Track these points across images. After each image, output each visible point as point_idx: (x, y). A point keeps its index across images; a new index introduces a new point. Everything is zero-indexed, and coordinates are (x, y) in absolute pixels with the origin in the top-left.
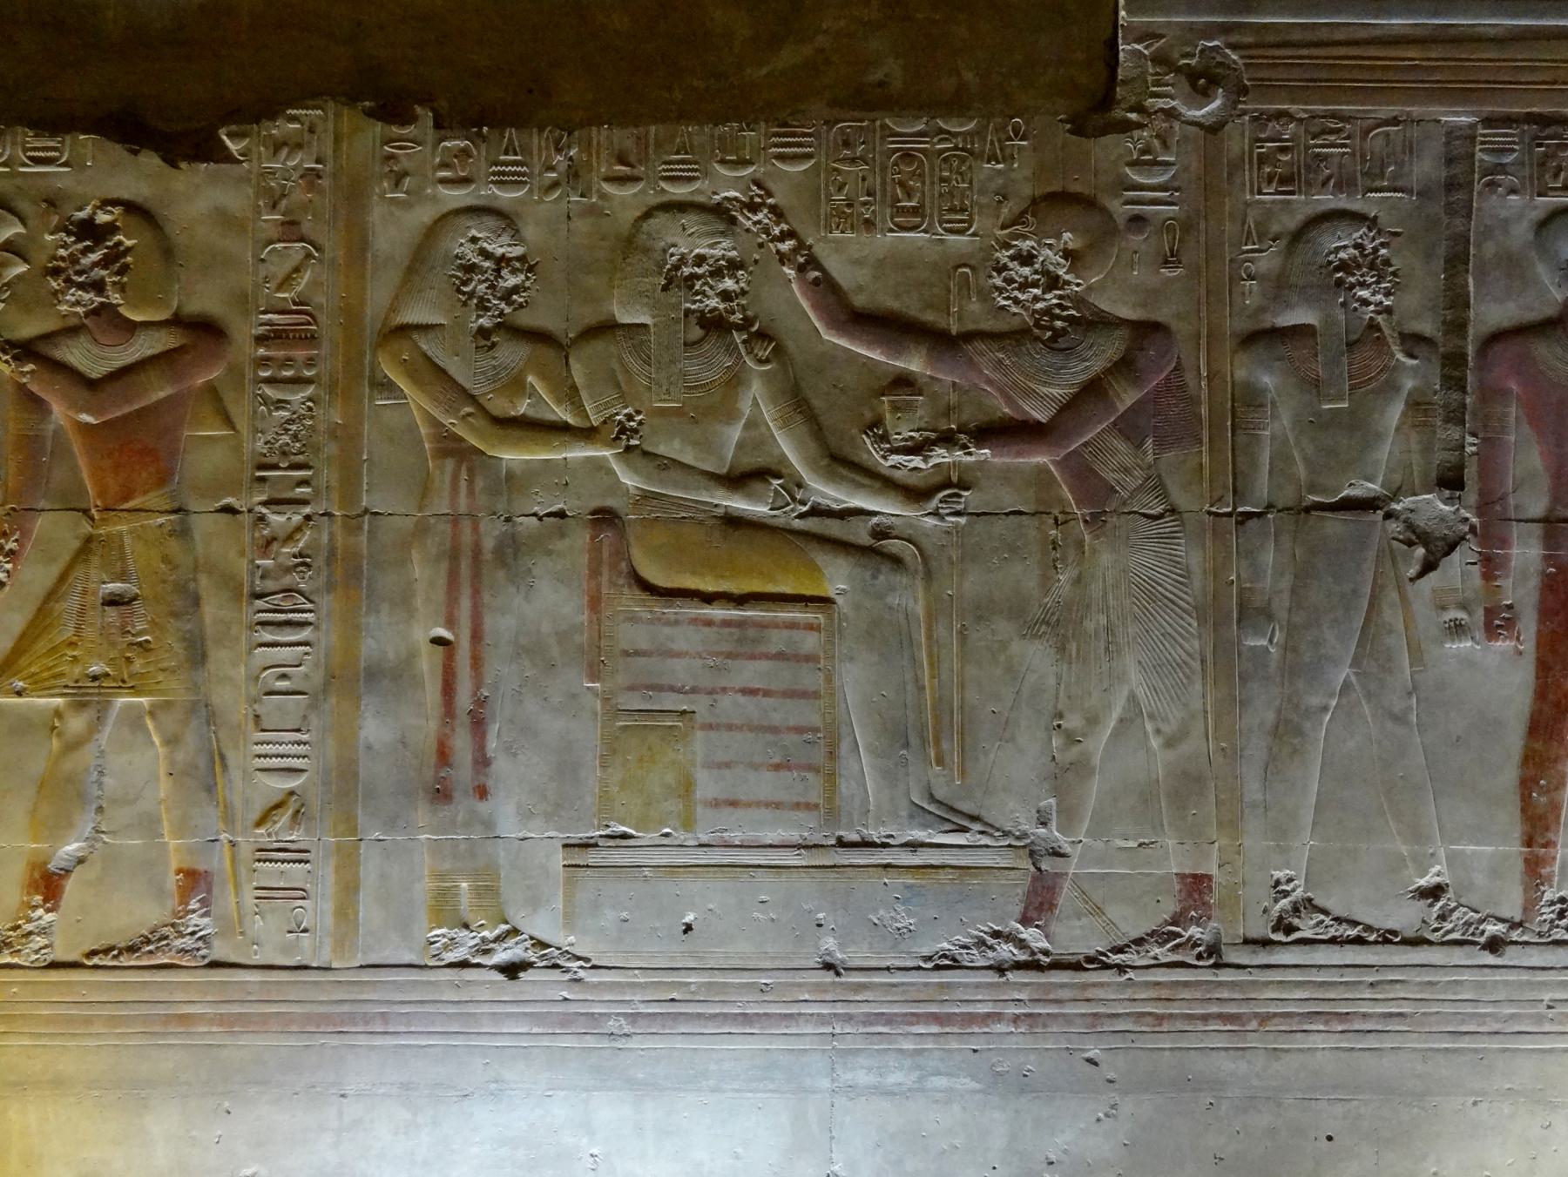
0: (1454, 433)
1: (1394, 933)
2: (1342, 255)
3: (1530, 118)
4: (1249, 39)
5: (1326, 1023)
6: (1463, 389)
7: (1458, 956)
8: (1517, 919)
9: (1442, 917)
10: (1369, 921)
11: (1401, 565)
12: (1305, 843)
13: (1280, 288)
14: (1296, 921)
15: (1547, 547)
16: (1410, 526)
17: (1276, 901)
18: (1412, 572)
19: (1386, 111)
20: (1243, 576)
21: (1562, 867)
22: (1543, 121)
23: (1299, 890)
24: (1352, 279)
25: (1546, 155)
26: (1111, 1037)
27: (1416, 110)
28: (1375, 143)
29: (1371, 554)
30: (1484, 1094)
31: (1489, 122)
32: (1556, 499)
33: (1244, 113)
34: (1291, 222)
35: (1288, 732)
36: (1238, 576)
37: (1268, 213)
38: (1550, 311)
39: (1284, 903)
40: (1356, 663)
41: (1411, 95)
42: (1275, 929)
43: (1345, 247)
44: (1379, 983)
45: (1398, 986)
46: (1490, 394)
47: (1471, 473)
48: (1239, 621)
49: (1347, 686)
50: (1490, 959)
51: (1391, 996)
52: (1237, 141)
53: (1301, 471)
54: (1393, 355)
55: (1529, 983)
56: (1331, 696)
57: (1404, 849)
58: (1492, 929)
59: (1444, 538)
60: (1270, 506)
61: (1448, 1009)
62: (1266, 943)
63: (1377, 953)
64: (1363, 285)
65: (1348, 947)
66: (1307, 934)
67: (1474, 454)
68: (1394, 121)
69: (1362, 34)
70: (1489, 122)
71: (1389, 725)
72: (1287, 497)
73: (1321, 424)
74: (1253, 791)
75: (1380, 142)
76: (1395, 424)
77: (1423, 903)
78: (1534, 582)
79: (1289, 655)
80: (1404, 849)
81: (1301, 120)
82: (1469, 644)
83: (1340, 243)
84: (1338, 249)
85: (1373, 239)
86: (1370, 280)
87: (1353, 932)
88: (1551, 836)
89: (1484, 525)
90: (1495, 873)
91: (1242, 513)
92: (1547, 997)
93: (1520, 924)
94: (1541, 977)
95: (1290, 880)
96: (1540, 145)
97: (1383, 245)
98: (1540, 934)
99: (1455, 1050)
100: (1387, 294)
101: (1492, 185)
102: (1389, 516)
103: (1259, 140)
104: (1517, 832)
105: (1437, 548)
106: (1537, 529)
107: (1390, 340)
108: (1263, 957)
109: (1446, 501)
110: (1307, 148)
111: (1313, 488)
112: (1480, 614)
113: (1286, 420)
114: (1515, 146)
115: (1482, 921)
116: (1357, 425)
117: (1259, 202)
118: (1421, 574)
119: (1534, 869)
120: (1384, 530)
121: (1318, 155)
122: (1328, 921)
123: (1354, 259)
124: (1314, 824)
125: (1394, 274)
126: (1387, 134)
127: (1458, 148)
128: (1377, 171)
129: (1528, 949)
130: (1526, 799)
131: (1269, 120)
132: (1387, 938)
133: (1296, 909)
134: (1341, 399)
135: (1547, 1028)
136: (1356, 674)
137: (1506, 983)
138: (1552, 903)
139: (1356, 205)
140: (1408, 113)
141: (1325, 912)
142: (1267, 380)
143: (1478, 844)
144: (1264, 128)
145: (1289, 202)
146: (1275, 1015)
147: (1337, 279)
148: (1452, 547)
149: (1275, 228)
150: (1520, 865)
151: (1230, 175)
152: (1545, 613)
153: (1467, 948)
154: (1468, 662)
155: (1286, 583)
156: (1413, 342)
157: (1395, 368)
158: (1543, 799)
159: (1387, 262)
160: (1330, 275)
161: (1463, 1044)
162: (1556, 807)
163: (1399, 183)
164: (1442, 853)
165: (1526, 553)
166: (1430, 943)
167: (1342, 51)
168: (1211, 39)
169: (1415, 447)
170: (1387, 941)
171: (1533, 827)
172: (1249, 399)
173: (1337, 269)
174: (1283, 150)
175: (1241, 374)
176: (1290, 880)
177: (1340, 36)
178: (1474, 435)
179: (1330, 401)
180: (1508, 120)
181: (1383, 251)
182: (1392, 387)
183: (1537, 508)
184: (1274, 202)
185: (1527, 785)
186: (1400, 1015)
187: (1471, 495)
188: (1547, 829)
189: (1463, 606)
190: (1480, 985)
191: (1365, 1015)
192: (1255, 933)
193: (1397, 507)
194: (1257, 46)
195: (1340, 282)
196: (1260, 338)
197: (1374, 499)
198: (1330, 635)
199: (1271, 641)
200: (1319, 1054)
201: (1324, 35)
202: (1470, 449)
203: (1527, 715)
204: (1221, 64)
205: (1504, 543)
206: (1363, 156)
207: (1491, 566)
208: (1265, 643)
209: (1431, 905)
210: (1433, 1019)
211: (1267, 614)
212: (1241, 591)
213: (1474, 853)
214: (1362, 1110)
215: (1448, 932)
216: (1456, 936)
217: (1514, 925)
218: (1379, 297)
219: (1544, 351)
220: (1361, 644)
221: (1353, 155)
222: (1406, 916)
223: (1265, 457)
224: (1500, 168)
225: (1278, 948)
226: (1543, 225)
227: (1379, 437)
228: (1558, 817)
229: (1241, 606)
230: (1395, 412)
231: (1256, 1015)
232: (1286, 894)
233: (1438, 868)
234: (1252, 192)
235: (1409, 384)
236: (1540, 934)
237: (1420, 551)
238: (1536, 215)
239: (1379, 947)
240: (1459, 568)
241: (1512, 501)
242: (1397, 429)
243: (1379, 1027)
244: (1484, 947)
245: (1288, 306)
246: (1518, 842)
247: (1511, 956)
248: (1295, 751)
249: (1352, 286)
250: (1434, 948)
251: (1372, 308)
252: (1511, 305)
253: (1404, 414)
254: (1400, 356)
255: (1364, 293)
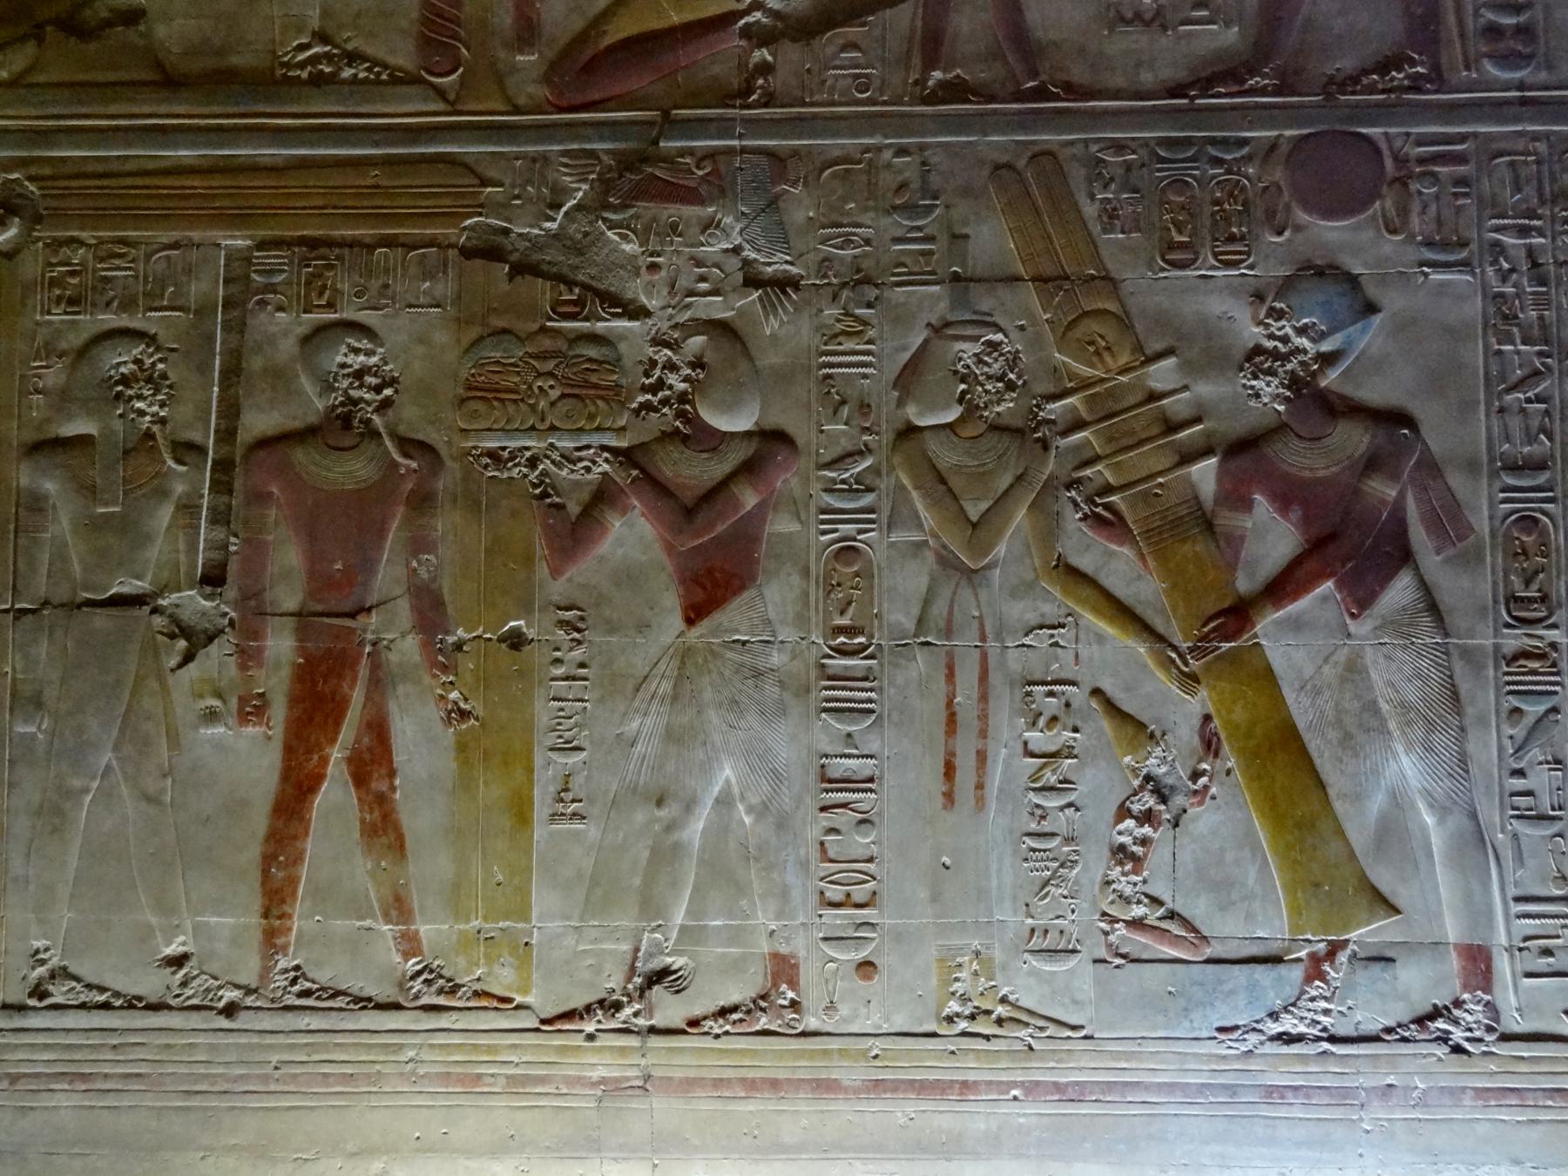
0: (220, 533)
1: (140, 999)
2: (123, 370)
3: (302, 241)
4: (47, 171)
5: (71, 1083)
6: (230, 492)
7: (195, 1020)
8: (253, 986)
9: (184, 984)
10: (118, 987)
11: (164, 657)
12: (65, 916)
13: (63, 400)
14: (51, 987)
15: (300, 640)
16: (174, 620)
17: (33, 968)
18: (173, 663)
19: (166, 236)
20: (18, 667)
21: (297, 941)
22: (313, 243)
23: (55, 959)
24: (130, 392)
25: (312, 275)
26: (79, 1095)
27: (196, 235)
28: (158, 264)
29: (137, 646)
30: (213, 1149)
31: (261, 245)
32: (311, 594)
33: (38, 239)
34: (75, 340)
35: (53, 814)
36: (14, 669)
37: (58, 333)
38: (312, 419)
39: (41, 971)
40: (117, 748)
41: (193, 221)
42: (30, 995)
43: (125, 363)
44: (121, 1045)
45: (138, 1048)
46: (260, 498)
47: (233, 567)
48: (12, 710)
49: (108, 768)
50: (224, 1023)
51: (131, 1057)
52: (31, 266)
53: (77, 568)
54: (164, 462)
55: (260, 1046)
56: (94, 778)
57: (154, 920)
58: (230, 995)
59: (205, 631)
60: (46, 603)
61: (184, 1070)
62: (21, 1008)
63: (122, 1018)
64: (140, 397)
65: (95, 1012)
66: (58, 999)
67: (236, 553)
68: (175, 246)
69: (151, 166)
70: (261, 245)
71: (143, 805)
72: (62, 594)
73: (94, 526)
74: (17, 866)
75: (161, 267)
76: (165, 524)
77: (169, 970)
78: (285, 673)
79: (56, 741)
80: (154, 920)
81: (90, 246)
82: (222, 730)
83: (121, 359)
84: (119, 364)
85: (151, 355)
86: (146, 393)
87: (102, 998)
88: (287, 909)
89: (243, 618)
90: (235, 942)
91: (20, 610)
92: (275, 1058)
93: (255, 991)
94: (270, 1040)
95: (47, 950)
96: (308, 266)
97: (161, 360)
98: (273, 1001)
99: (188, 1109)
100: (162, 405)
101: (262, 303)
102: (155, 611)
103: (52, 265)
104: (257, 904)
105: (196, 639)
106: (290, 622)
107: (163, 449)
108: (18, 1022)
109: (206, 597)
110: (95, 270)
111: (86, 589)
112: (234, 702)
113: (65, 522)
114: (281, 267)
115: (220, 988)
116: (128, 529)
117: (50, 323)
118: (180, 666)
119: (272, 940)
120: (149, 624)
121: (105, 277)
122: (79, 987)
123: (133, 374)
124: (72, 896)
125: (170, 387)
126: (168, 257)
127: (239, 272)
128: (158, 292)
129: (260, 1014)
130: (266, 872)
131: (60, 246)
132: (132, 1004)
133: (53, 976)
134: (115, 503)
135: (272, 1088)
136: (118, 759)
137: (238, 1045)
138: (286, 971)
139: (136, 323)
140: (190, 239)
141: (77, 979)
142: (50, 486)
143: (220, 915)
144: (56, 252)
145: (74, 321)
146: (25, 1075)
147: (117, 391)
148: (211, 639)
149: (64, 345)
150: (256, 937)
151: (24, 297)
152: (294, 701)
153: (204, 1013)
154: (219, 746)
155: (55, 676)
156: (187, 450)
157: (166, 474)
158: (281, 875)
159: (164, 376)
160: (111, 388)
161: (195, 1102)
162: (293, 882)
163: (178, 303)
164: (188, 925)
165: (281, 645)
166: (170, 1008)
167: (129, 181)
168: (11, 171)
169: (182, 546)
170: (131, 1007)
171: (271, 900)
172: (36, 504)
173: (117, 383)
174: (73, 274)
175: (24, 481)
176: (47, 950)
177: (129, 167)
178: (236, 536)
179: (106, 504)
180: (278, 243)
181: (160, 366)
182: (163, 493)
183: (291, 603)
184: (62, 321)
185: (268, 860)
186: (138, 1075)
187: (231, 591)
188: (283, 901)
189: (219, 695)
190: (213, 1048)
191: (106, 1076)
192: (12, 999)
193: (163, 602)
194: (52, 178)
195: (119, 396)
196: (46, 447)
197: (144, 595)
198: (93, 724)
199: (39, 728)
200: (63, 1112)
201: (115, 167)
202: (233, 548)
203: (272, 796)
204: (20, 195)
205: (256, 635)
206: (146, 277)
207: (248, 656)
208: (33, 729)
209: (174, 973)
210: (168, 1079)
211: (37, 703)
212: (14, 680)
213: (218, 924)
214: (99, 1164)
215: (189, 998)
216: (195, 1001)
217: (249, 991)
218: (155, 408)
219: (300, 455)
220: (122, 731)
221: (136, 277)
222: (151, 983)
223: (44, 558)
224: (271, 288)
225: (31, 1013)
226: (306, 340)
227: (148, 538)
228: (294, 892)
229: (13, 696)
230: (165, 514)
231: (8, 1075)
232: (43, 962)
233: (182, 938)
234: (42, 314)
235: (179, 488)
236: (273, 1001)
237: (182, 644)
238: (301, 330)
239: (124, 1013)
240: (217, 659)
241: (268, 596)
242: (168, 528)
243: (119, 1087)
244: (220, 1012)
245: (70, 417)
246: (257, 915)
247: (243, 1020)
248: (55, 830)
249: (131, 398)
250: (174, 1013)
251: (148, 418)
252: (276, 414)
253: (174, 517)
254: (171, 463)
255: (139, 405)
